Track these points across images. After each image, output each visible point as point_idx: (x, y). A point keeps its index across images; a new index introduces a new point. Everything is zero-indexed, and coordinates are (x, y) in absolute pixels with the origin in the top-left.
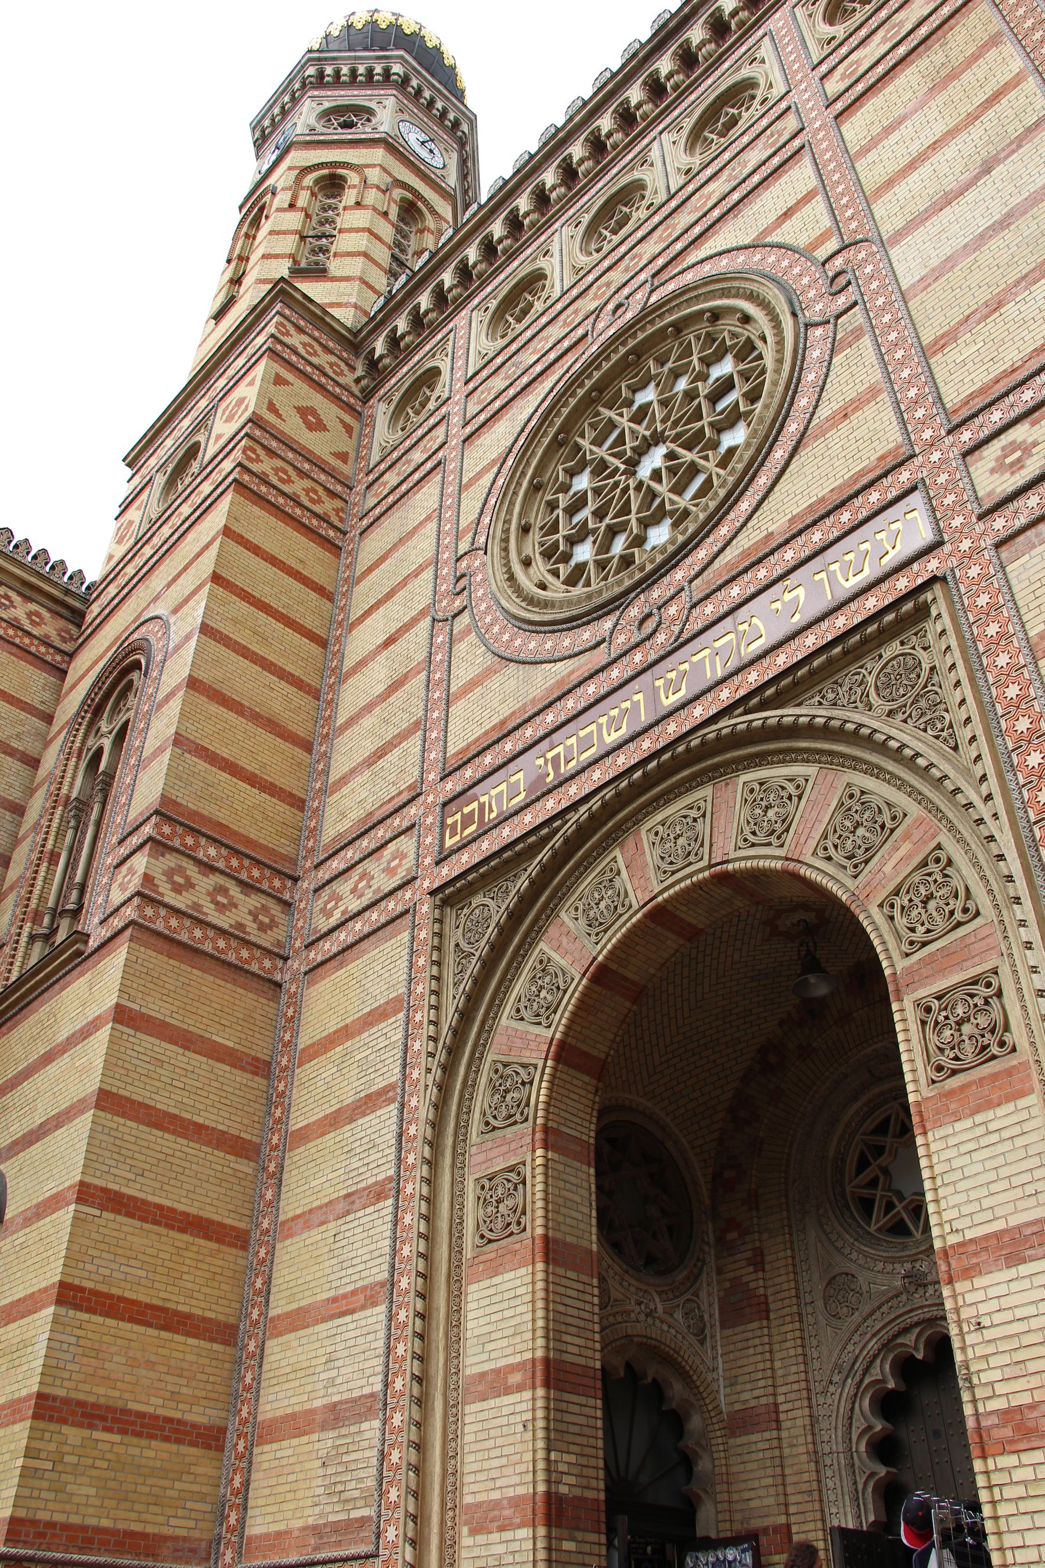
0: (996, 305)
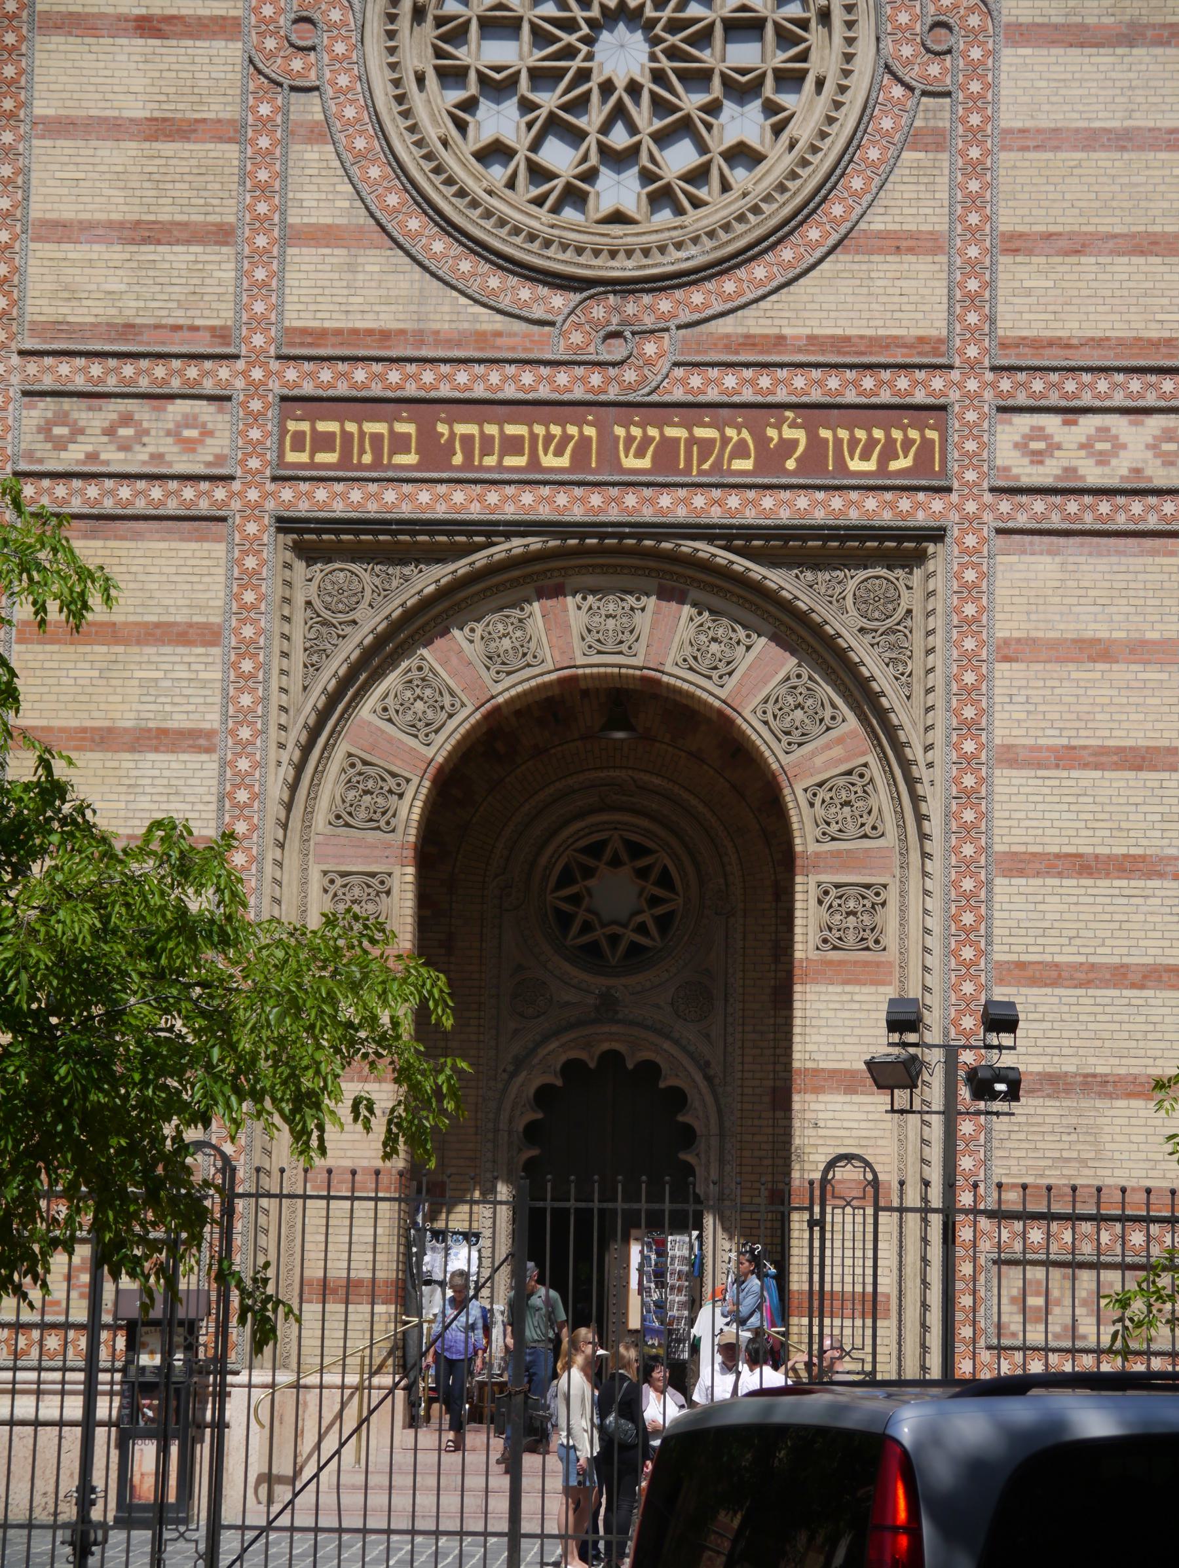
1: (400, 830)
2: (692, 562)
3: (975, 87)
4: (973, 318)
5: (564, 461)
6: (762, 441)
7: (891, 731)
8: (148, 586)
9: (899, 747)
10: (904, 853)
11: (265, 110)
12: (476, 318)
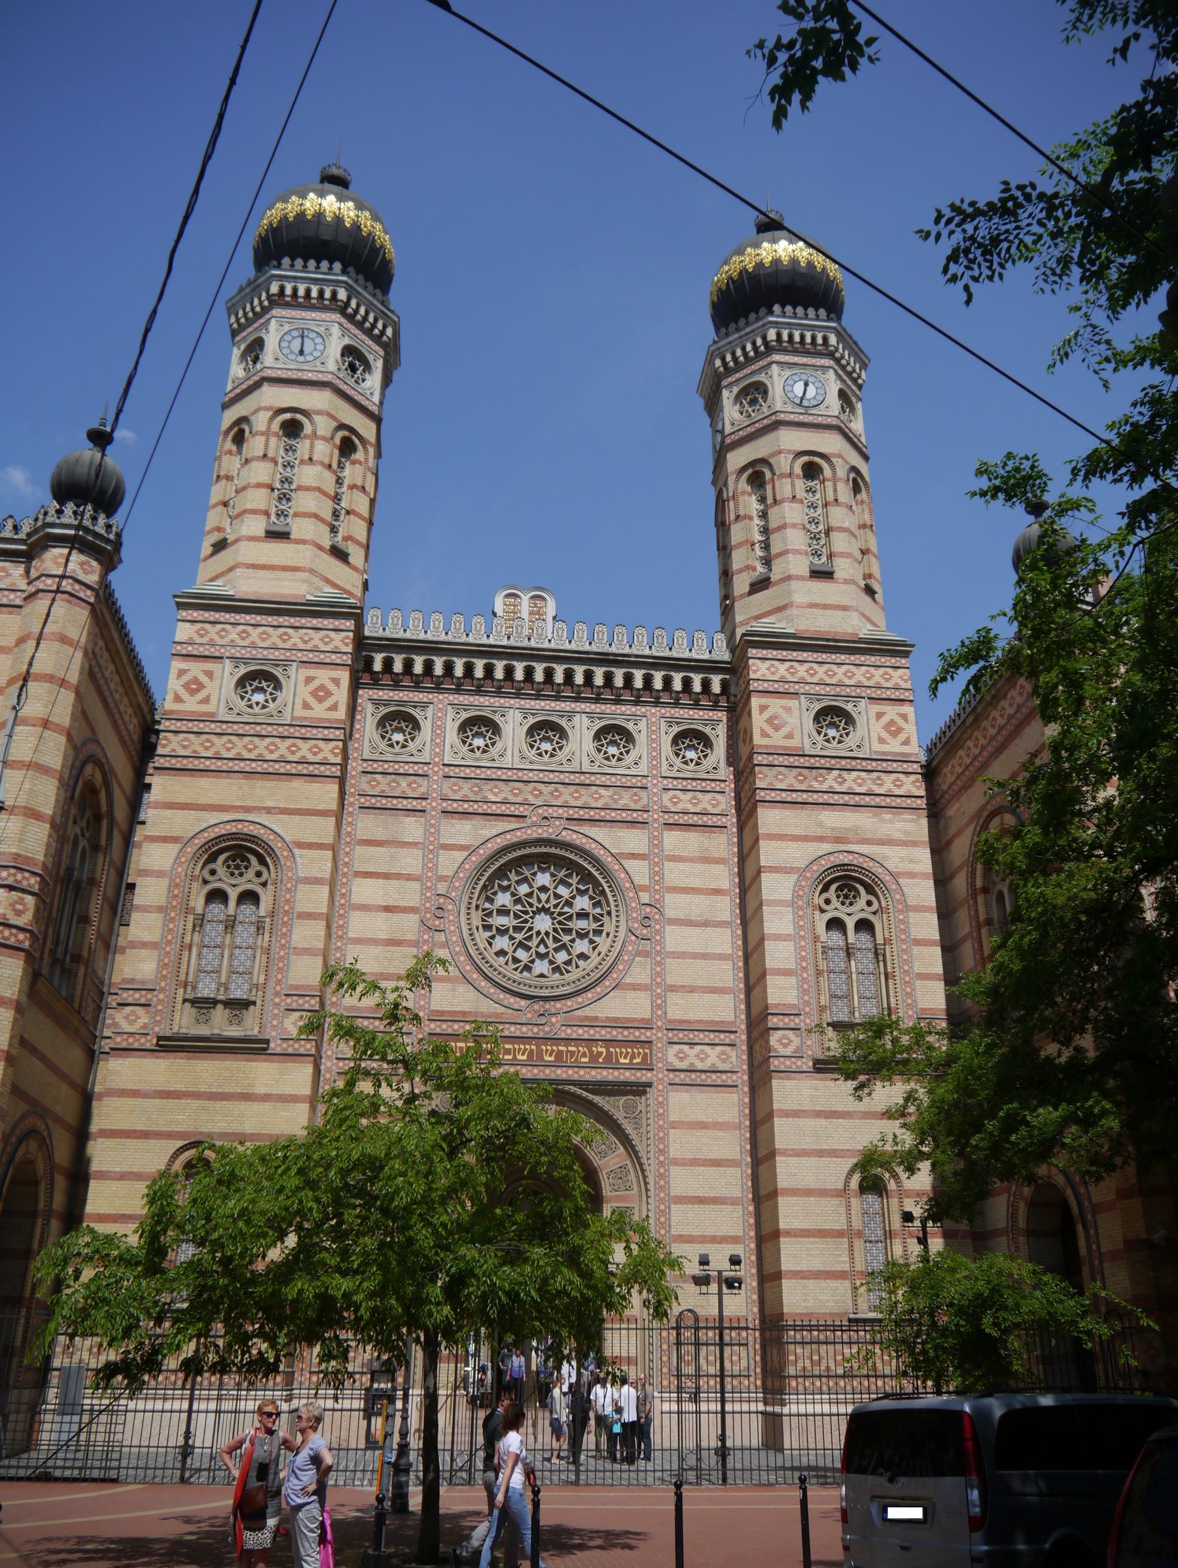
0: (692, 990)
2: (569, 1093)
3: (658, 938)
4: (659, 1012)
5: (525, 1057)
6: (591, 1052)
7: (636, 1153)
9: (638, 1158)
10: (640, 1196)
11: (426, 937)
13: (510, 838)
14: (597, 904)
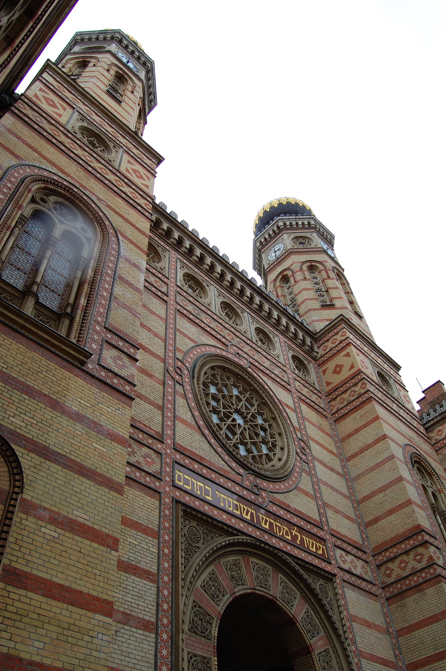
1: (213, 639)
6: (291, 533)
8: (134, 506)
12: (223, 465)
13: (218, 351)
14: (270, 426)
